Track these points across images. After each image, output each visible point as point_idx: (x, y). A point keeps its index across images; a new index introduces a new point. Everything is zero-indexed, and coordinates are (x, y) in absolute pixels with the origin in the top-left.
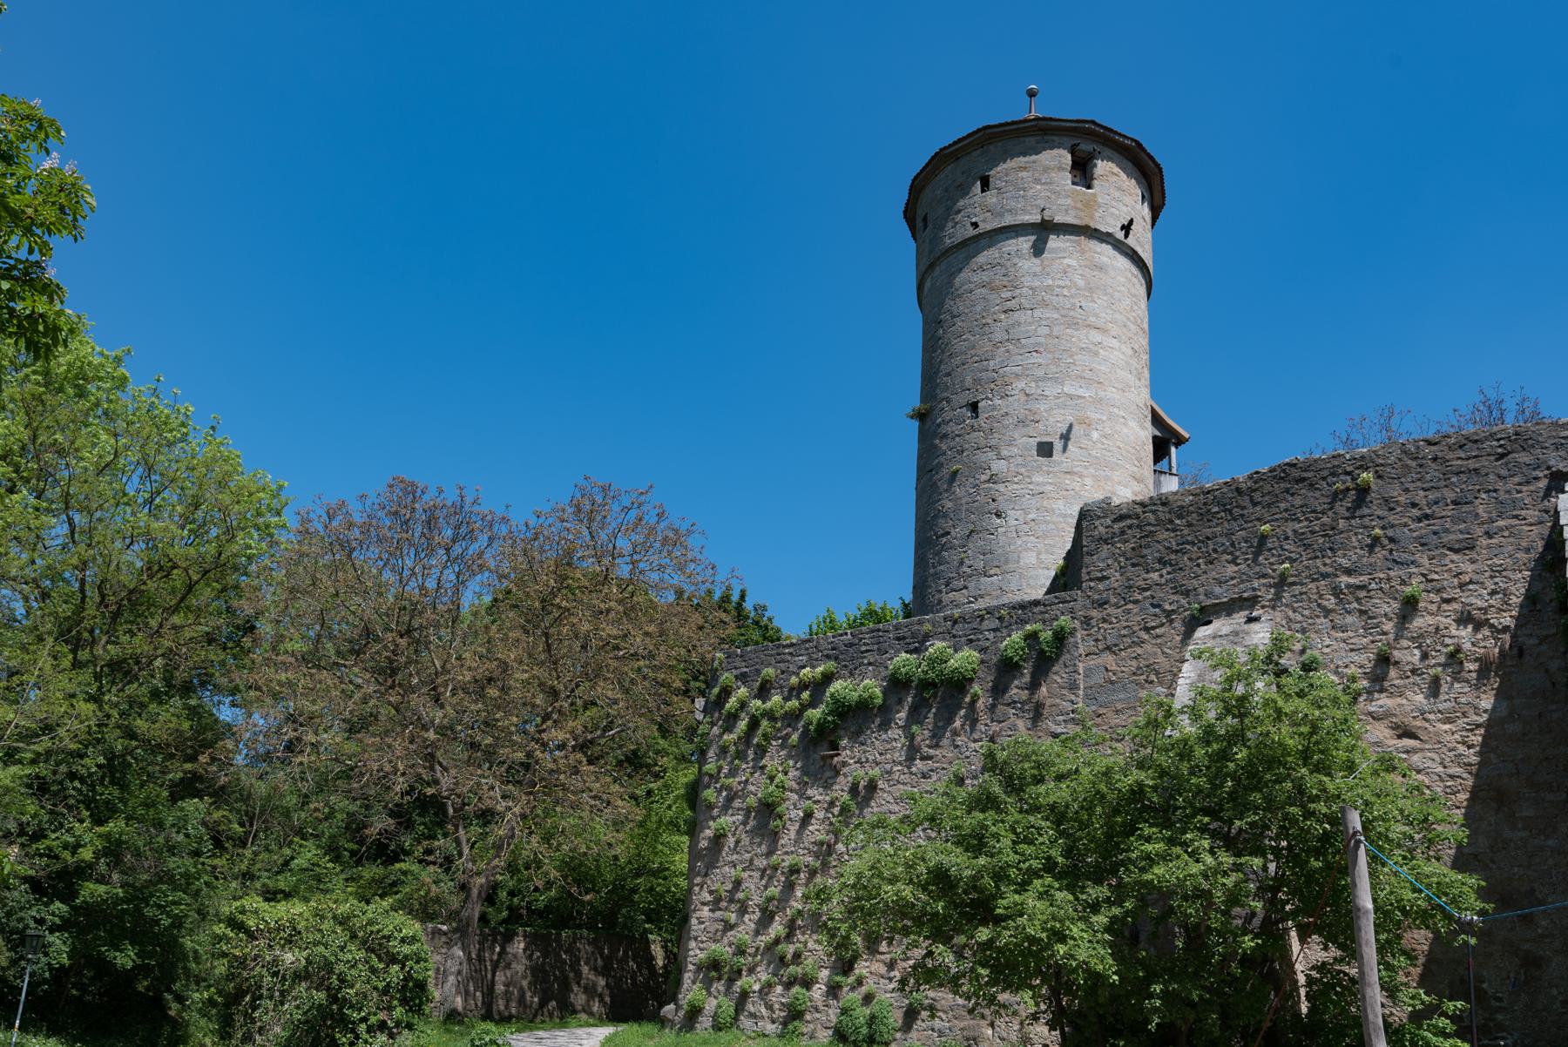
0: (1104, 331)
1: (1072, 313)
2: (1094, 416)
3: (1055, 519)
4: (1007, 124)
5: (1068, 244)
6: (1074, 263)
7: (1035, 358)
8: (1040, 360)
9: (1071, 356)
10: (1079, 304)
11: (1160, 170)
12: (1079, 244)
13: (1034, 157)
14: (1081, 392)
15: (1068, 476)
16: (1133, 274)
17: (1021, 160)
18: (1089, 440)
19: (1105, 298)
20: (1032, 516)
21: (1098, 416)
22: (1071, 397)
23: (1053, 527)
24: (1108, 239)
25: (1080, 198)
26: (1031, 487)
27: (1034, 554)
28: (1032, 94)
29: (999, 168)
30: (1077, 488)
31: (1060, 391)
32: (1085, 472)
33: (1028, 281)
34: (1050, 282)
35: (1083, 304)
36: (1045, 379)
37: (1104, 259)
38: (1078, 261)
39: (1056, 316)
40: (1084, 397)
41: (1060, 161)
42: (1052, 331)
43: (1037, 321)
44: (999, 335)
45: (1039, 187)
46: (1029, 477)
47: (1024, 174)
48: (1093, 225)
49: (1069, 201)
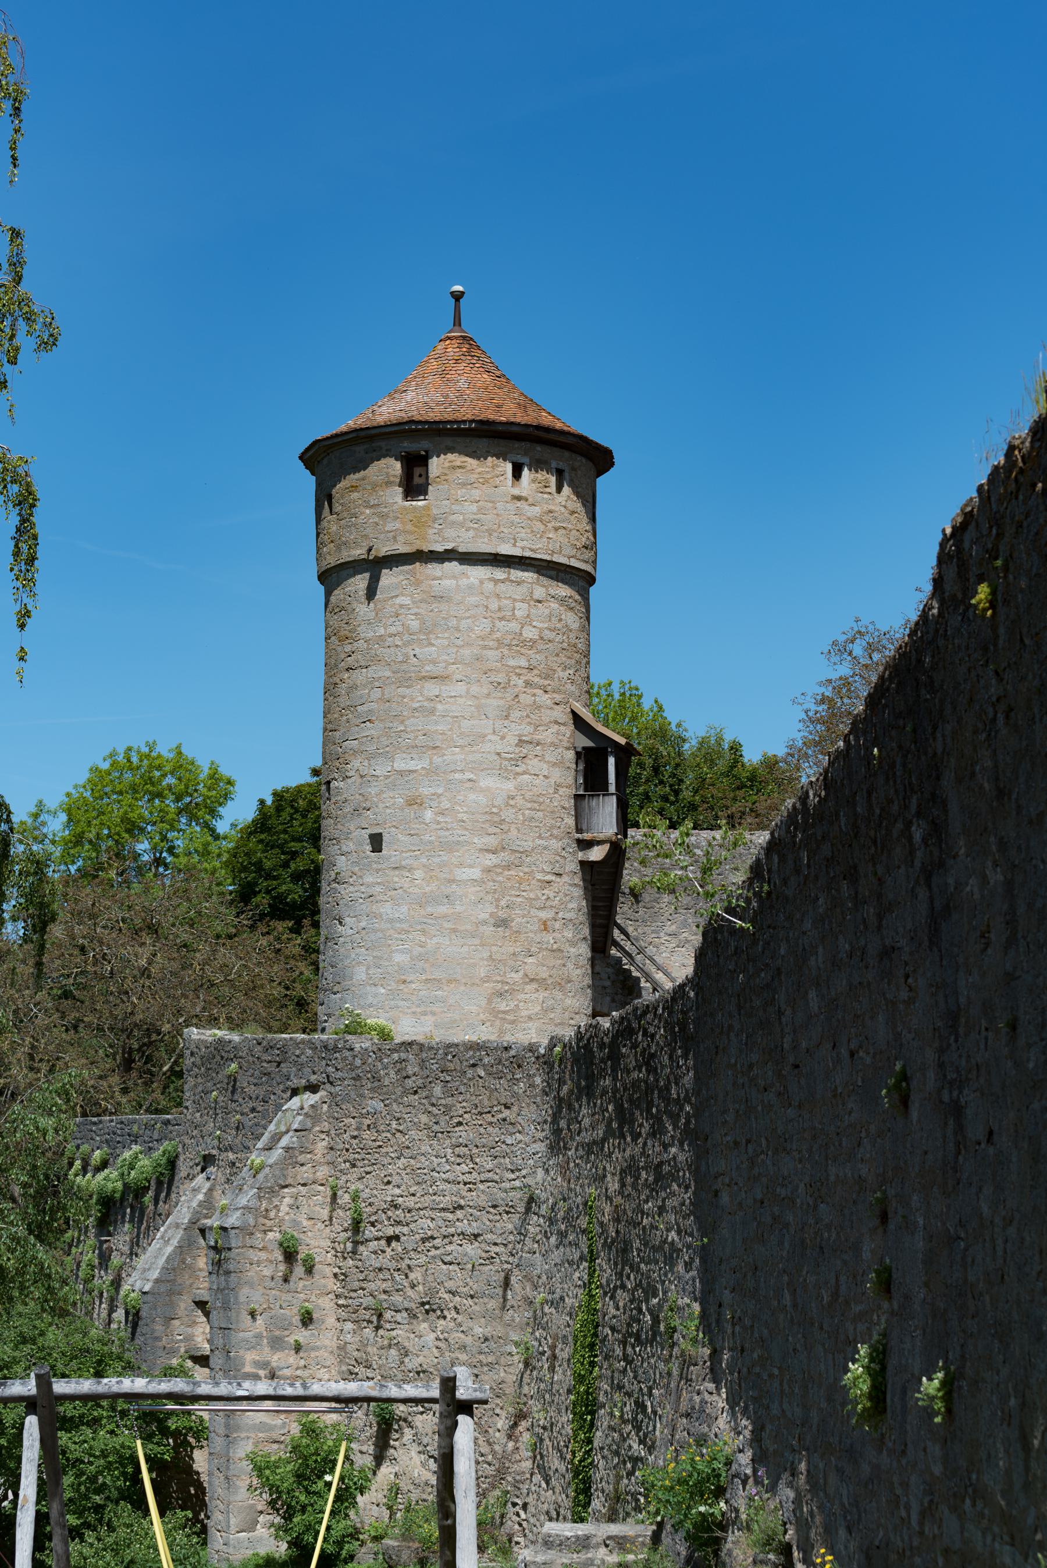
1: (404, 667)
2: (426, 791)
3: (384, 925)
4: (336, 435)
5: (402, 577)
6: (406, 600)
7: (370, 730)
8: (373, 732)
9: (402, 722)
10: (412, 653)
12: (413, 574)
13: (362, 472)
14: (412, 765)
15: (397, 873)
16: (496, 582)
17: (353, 478)
18: (420, 823)
19: (446, 635)
20: (363, 924)
22: (401, 773)
23: (381, 935)
24: (450, 556)
25: (410, 517)
26: (363, 888)
27: (364, 969)
28: (457, 297)
29: (338, 486)
30: (406, 885)
31: (389, 769)
32: (415, 864)
34: (382, 631)
35: (417, 651)
37: (447, 583)
38: (412, 598)
39: (388, 674)
41: (387, 473)
42: (383, 694)
43: (371, 683)
44: (344, 701)
45: (368, 511)
46: (361, 877)
48: (426, 548)
49: (398, 525)
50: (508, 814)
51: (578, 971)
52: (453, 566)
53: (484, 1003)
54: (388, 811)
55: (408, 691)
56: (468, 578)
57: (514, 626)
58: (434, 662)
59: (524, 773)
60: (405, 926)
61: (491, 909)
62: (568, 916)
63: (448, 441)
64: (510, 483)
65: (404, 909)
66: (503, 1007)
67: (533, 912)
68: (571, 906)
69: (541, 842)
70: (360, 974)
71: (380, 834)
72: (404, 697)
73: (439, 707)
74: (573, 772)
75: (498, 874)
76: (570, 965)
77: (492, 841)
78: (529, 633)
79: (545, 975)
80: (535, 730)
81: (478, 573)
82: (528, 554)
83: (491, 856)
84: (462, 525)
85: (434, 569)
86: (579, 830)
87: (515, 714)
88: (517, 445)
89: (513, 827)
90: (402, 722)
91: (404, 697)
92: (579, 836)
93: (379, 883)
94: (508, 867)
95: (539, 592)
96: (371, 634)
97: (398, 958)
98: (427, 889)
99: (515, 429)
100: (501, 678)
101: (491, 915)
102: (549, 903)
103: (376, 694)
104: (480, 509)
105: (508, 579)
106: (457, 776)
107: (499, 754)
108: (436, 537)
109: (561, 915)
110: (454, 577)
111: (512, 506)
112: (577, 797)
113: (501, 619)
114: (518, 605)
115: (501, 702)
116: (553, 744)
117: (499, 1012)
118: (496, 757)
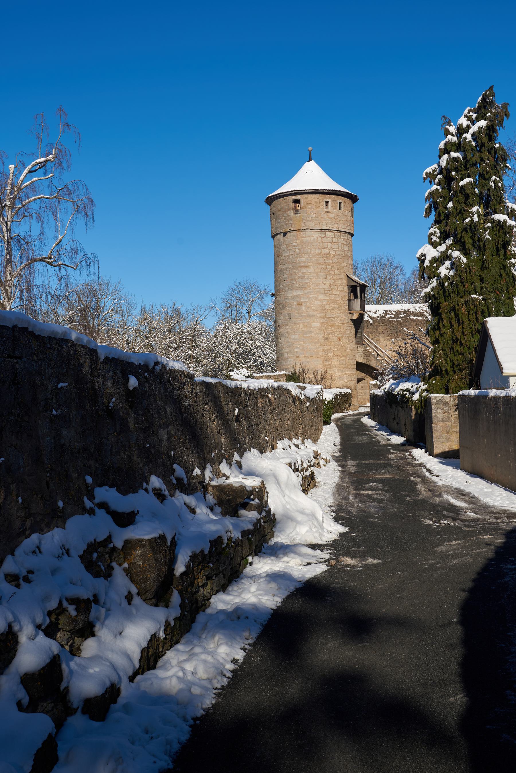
0: (307, 267)
2: (302, 300)
6: (295, 244)
9: (295, 280)
16: (322, 238)
34: (289, 254)
43: (286, 269)
47: (280, 213)
50: (327, 307)
51: (351, 352)
52: (309, 233)
53: (321, 362)
55: (297, 271)
56: (313, 237)
57: (327, 251)
58: (304, 262)
59: (332, 294)
60: (298, 341)
61: (322, 335)
62: (348, 335)
63: (306, 196)
64: (325, 208)
65: (297, 335)
66: (327, 363)
67: (336, 335)
68: (347, 333)
69: (338, 314)
70: (286, 355)
71: (290, 314)
72: (295, 273)
73: (306, 276)
74: (347, 293)
75: (324, 325)
76: (348, 350)
77: (323, 315)
78: (332, 252)
79: (340, 354)
80: (335, 281)
81: (316, 235)
82: (330, 229)
83: (323, 319)
84: (310, 221)
85: (302, 233)
86: (349, 310)
87: (329, 277)
88: (327, 196)
89: (329, 311)
90: (295, 280)
91: (295, 273)
92: (350, 312)
94: (328, 322)
95: (335, 240)
96: (285, 255)
97: (296, 350)
98: (304, 329)
99: (325, 191)
100: (325, 267)
101: (323, 337)
102: (340, 333)
103: (288, 272)
104: (316, 217)
105: (325, 237)
106: (312, 296)
107: (324, 289)
109: (344, 336)
110: (310, 237)
111: (326, 214)
112: (349, 301)
113: (324, 248)
114: (328, 244)
115: (324, 274)
116: (340, 285)
117: (326, 365)
118: (323, 290)
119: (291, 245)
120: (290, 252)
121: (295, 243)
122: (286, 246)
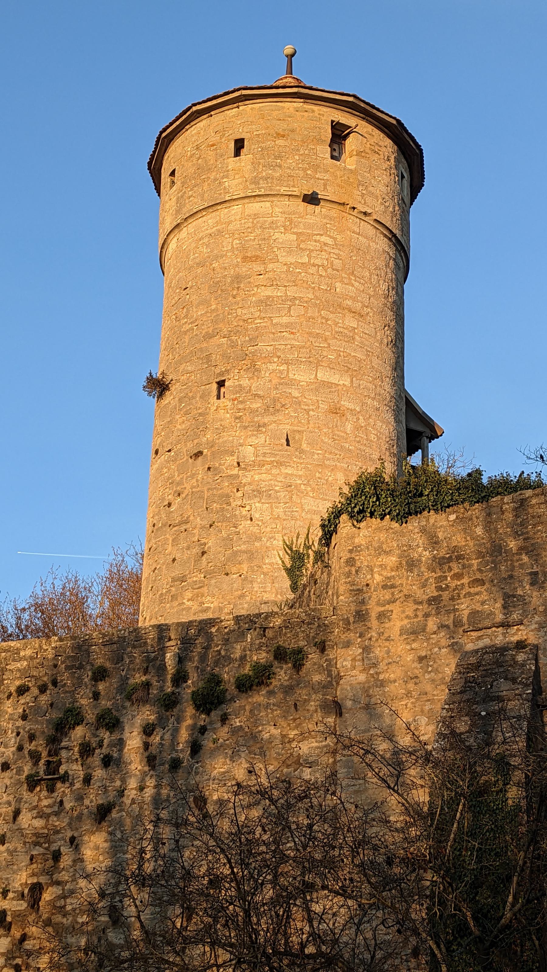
2: (346, 404)
6: (330, 241)
8: (293, 342)
9: (326, 340)
11: (421, 150)
14: (335, 379)
21: (351, 406)
33: (283, 257)
34: (305, 260)
36: (298, 362)
39: (311, 296)
40: (338, 385)
42: (306, 312)
47: (280, 142)
54: (311, 413)
58: (354, 299)
72: (327, 320)
91: (327, 320)
93: (300, 476)
108: (359, 198)
119: (318, 237)
120: (309, 257)
121: (331, 237)
122: (294, 237)
